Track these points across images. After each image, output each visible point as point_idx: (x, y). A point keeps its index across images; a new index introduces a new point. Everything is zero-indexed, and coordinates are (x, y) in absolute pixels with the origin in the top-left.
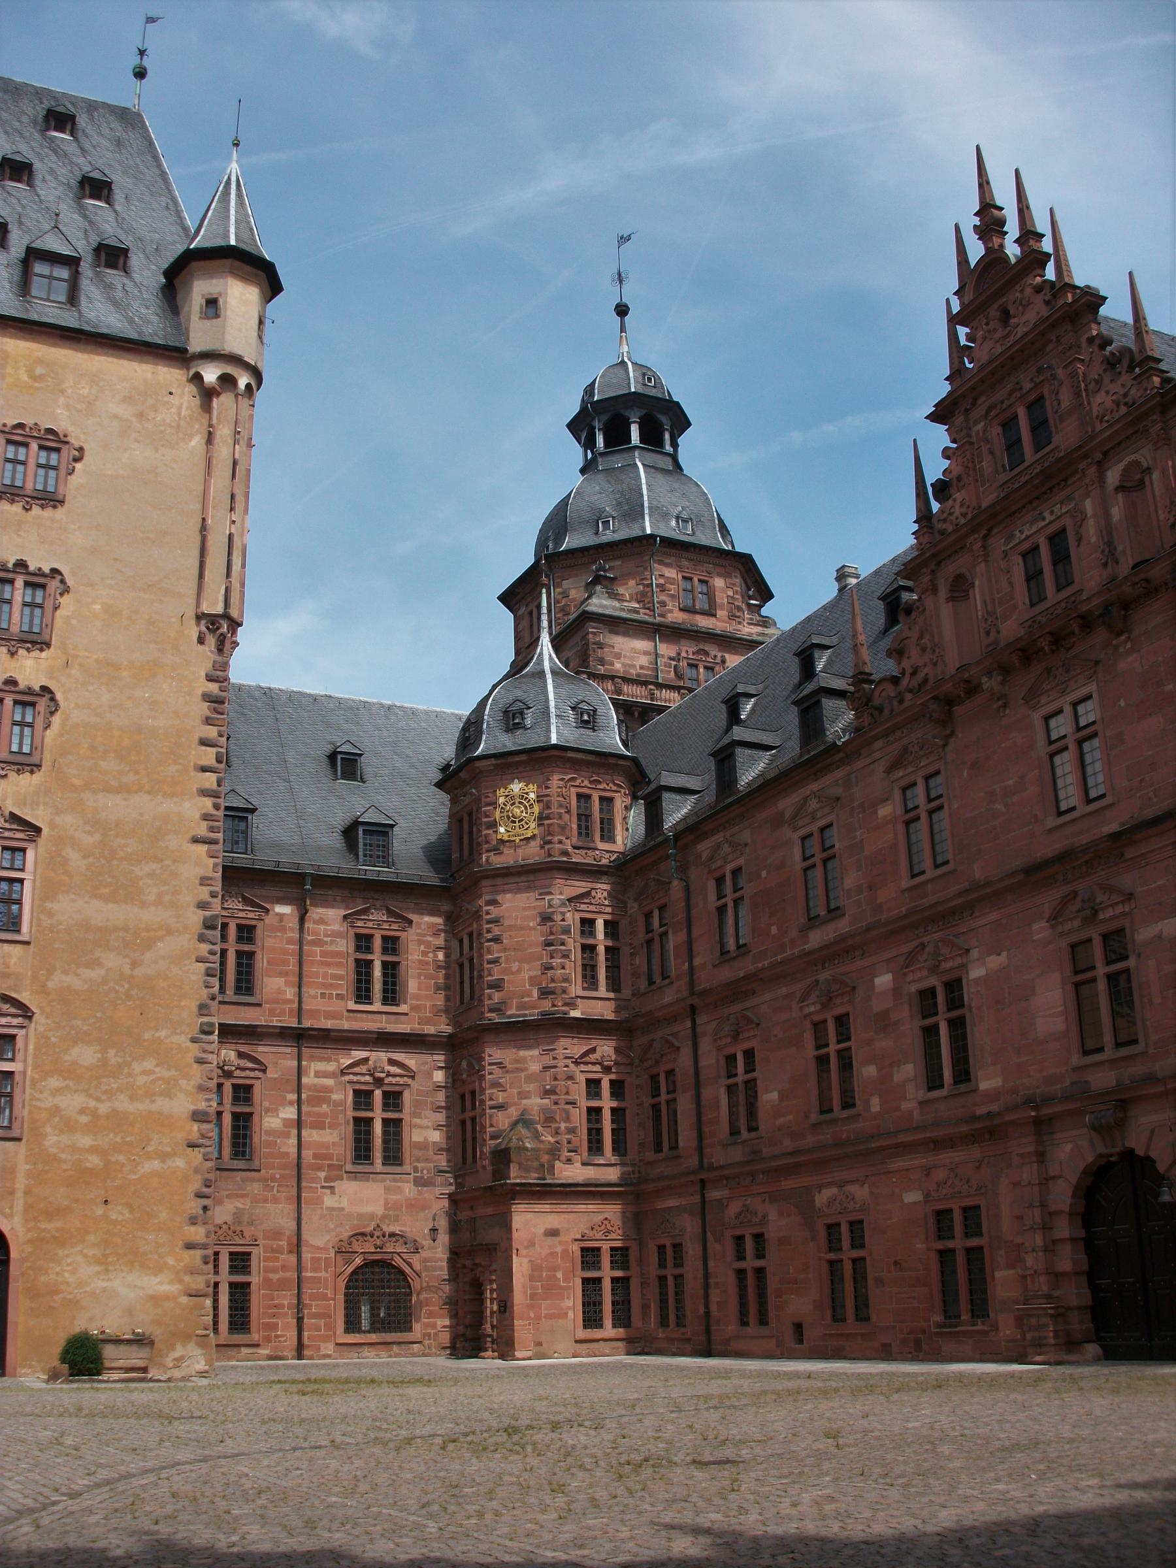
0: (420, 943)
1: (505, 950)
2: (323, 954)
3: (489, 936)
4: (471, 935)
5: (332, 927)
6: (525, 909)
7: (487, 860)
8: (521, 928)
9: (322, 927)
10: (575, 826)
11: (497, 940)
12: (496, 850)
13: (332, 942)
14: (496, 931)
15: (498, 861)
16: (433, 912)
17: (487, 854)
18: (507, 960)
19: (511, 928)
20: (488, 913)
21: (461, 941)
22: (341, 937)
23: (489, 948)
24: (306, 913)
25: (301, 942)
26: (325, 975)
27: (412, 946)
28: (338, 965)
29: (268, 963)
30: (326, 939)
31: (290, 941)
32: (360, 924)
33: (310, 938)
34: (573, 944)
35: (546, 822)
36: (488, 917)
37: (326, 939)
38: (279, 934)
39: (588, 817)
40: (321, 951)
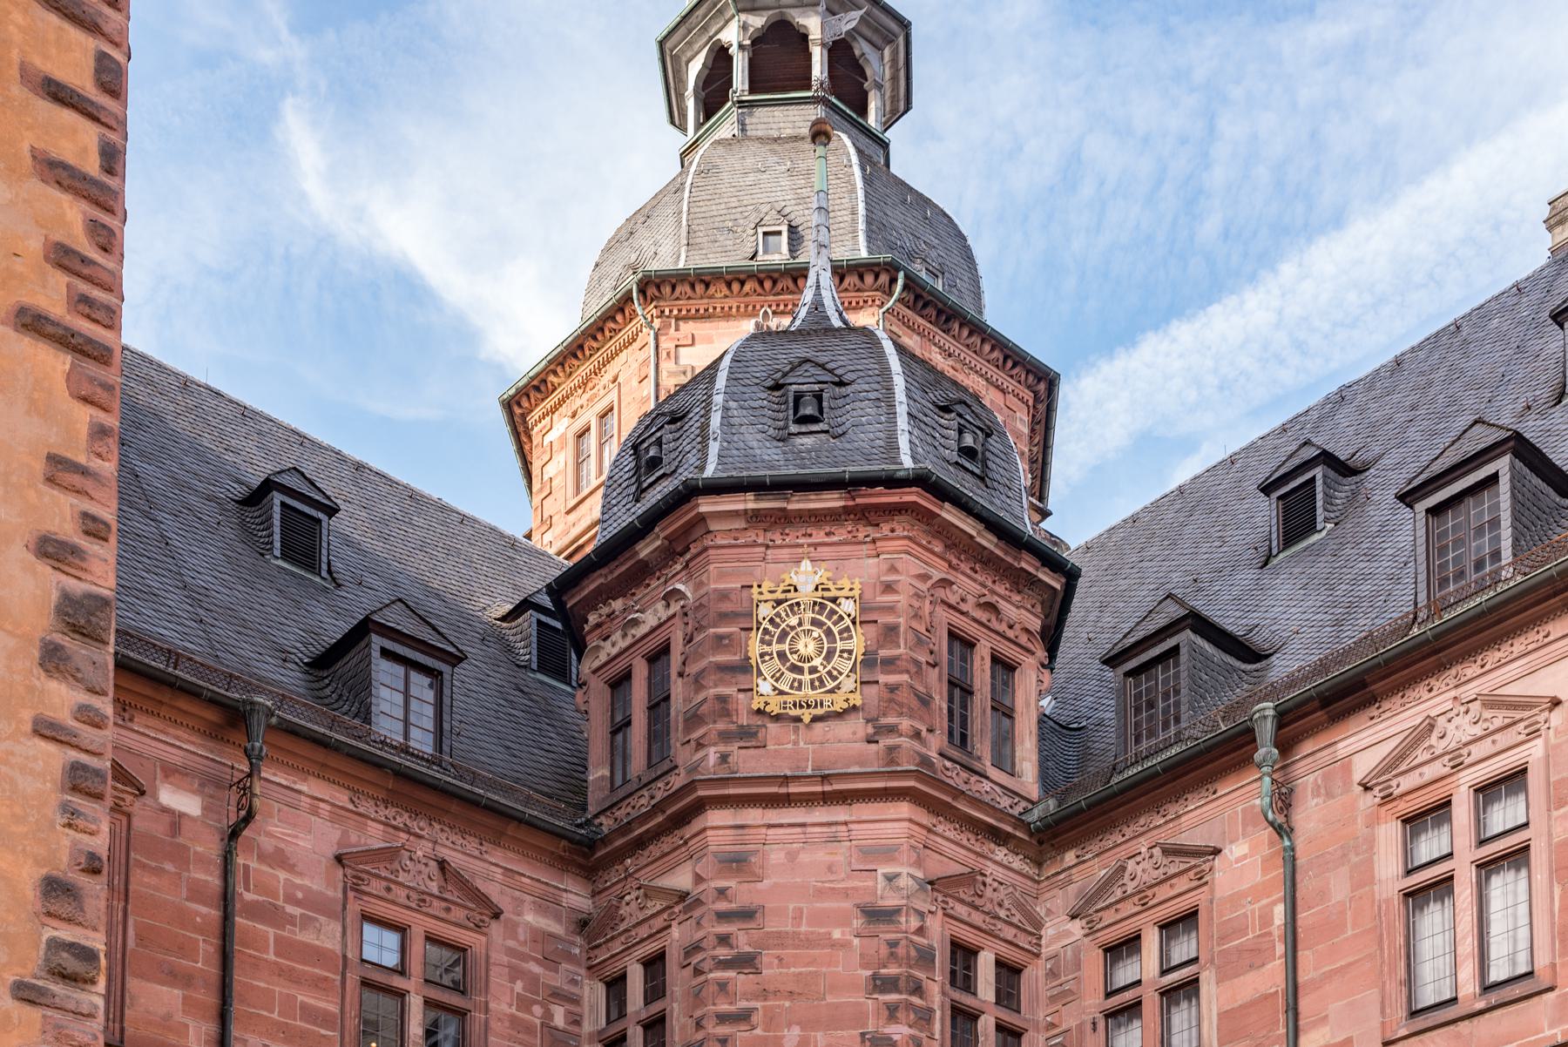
0: (515, 974)
1: (764, 994)
2: (283, 947)
3: (723, 953)
4: (655, 964)
5: (307, 882)
6: (820, 893)
7: (724, 758)
8: (809, 942)
9: (282, 875)
10: (945, 706)
11: (746, 962)
12: (746, 735)
13: (306, 922)
14: (743, 944)
15: (748, 762)
16: (548, 903)
17: (722, 748)
18: (771, 1021)
19: (781, 939)
20: (722, 893)
21: (616, 985)
22: (330, 915)
23: (723, 986)
24: (248, 819)
25: (226, 900)
26: (288, 1004)
27: (498, 978)
28: (318, 984)
29: (140, 938)
30: (290, 909)
31: (196, 893)
32: (376, 887)
33: (249, 896)
34: (937, 993)
35: (883, 679)
36: (722, 906)
37: (290, 909)
38: (169, 867)
39: (968, 692)
40: (278, 939)
